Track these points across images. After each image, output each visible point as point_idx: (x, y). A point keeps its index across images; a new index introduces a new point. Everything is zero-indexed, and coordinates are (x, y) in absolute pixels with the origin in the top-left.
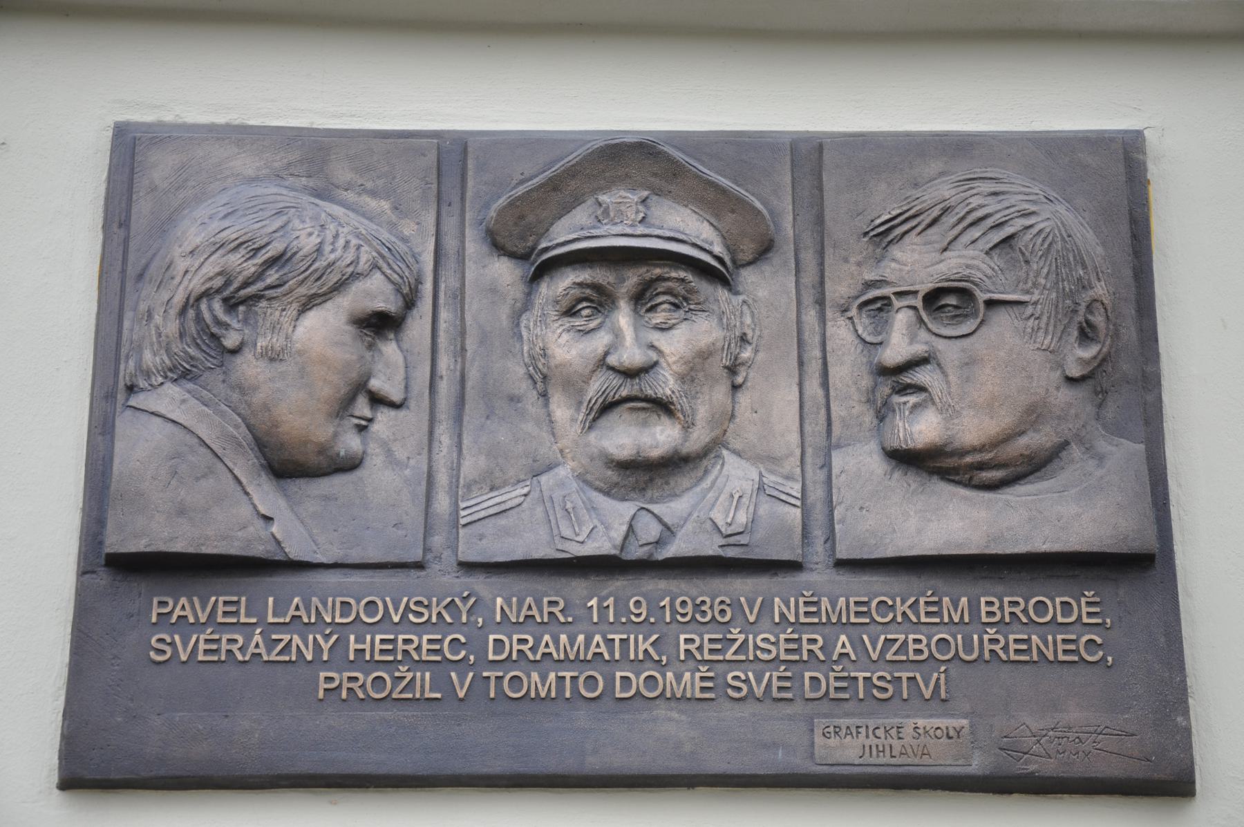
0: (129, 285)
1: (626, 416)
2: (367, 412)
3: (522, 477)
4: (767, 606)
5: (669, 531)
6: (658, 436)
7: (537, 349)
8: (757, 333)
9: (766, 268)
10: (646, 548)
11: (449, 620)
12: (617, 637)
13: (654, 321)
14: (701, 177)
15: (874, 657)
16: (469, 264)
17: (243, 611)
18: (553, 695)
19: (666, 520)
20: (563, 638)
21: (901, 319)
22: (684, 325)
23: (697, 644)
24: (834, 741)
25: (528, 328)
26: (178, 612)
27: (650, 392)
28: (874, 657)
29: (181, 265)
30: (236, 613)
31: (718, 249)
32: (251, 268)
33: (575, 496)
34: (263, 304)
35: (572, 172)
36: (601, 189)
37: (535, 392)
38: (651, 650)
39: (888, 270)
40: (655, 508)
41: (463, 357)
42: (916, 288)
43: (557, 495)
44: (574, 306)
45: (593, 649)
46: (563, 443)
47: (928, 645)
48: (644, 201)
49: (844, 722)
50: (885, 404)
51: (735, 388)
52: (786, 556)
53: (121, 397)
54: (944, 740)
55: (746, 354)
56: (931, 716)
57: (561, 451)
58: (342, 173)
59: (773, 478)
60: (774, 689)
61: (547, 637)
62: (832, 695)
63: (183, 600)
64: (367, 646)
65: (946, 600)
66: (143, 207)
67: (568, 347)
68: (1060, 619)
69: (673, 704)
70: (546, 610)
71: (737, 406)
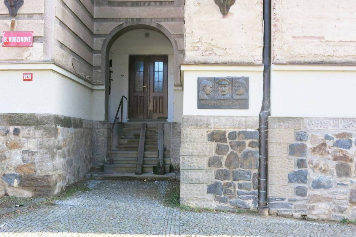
5: (225, 98)
21: (236, 87)
39: (236, 84)
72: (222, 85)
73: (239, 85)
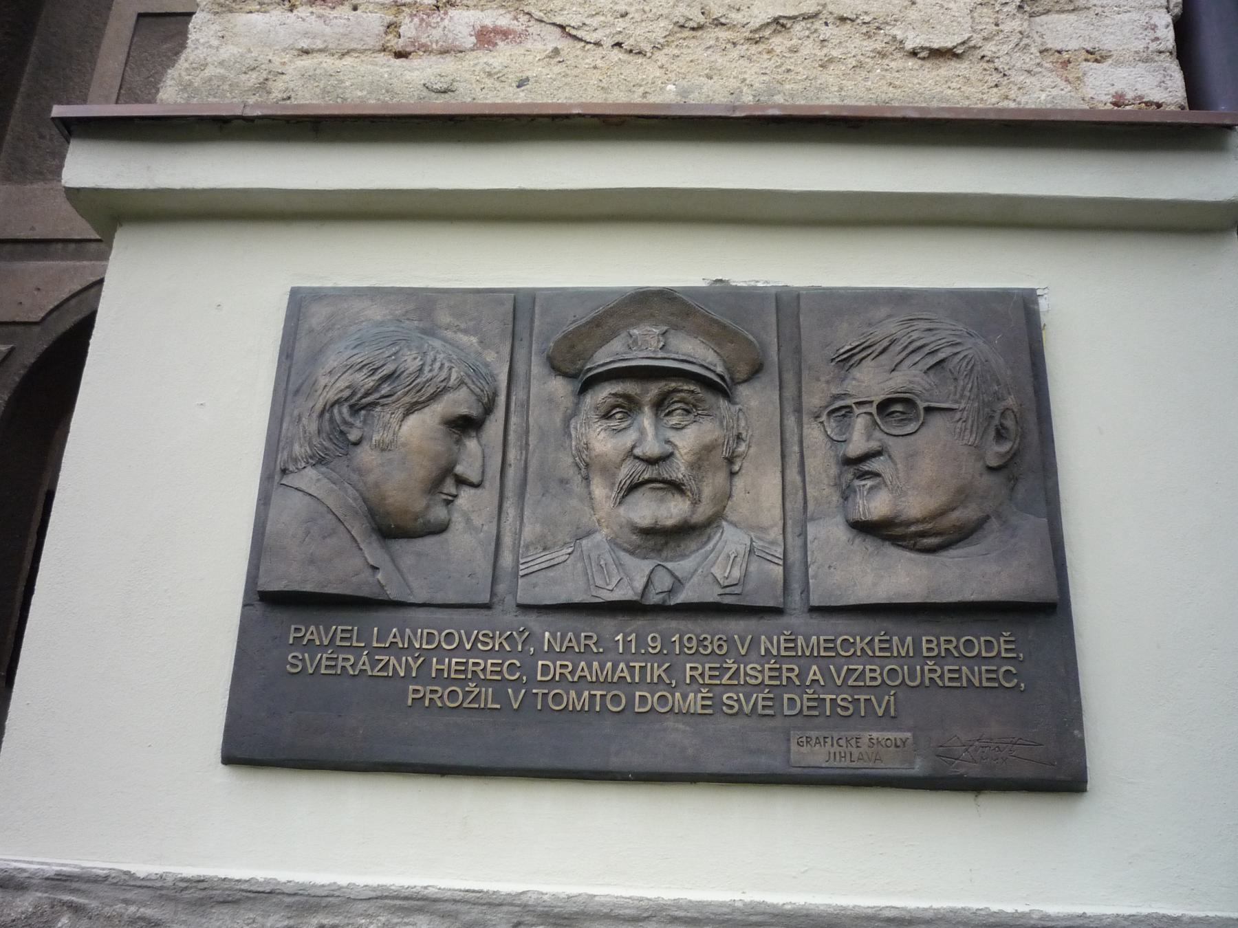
0: (289, 397)
1: (649, 494)
2: (453, 491)
4: (755, 643)
5: (678, 583)
8: (750, 433)
9: (757, 384)
10: (661, 596)
11: (508, 649)
12: (637, 665)
15: (839, 683)
16: (534, 383)
17: (355, 638)
18: (586, 708)
19: (677, 574)
20: (595, 664)
21: (860, 423)
22: (694, 427)
23: (700, 671)
24: (805, 749)
26: (308, 636)
27: (666, 476)
28: (839, 683)
29: (323, 381)
30: (350, 638)
31: (720, 369)
32: (370, 383)
33: (607, 556)
34: (379, 409)
35: (610, 313)
36: (633, 325)
38: (663, 675)
39: (850, 386)
40: (669, 565)
41: (527, 450)
42: (872, 398)
43: (594, 555)
45: (618, 674)
46: (601, 514)
47: (881, 674)
48: (664, 334)
49: (813, 734)
50: (849, 487)
52: (771, 604)
53: (277, 478)
54: (893, 748)
55: (742, 448)
56: (883, 730)
57: (599, 521)
58: (444, 318)
59: (761, 543)
60: (760, 707)
61: (583, 664)
62: (806, 712)
63: (312, 628)
64: (445, 667)
65: (895, 638)
66: (303, 345)
67: (604, 441)
68: (984, 654)
69: (680, 717)
70: (583, 641)
72: (630, 387)
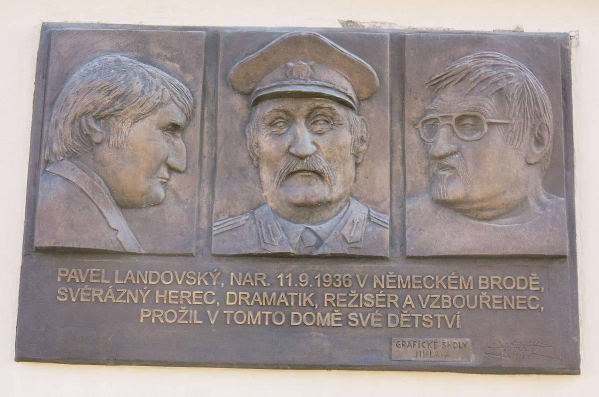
0: (47, 108)
2: (167, 176)
3: (245, 210)
4: (371, 280)
5: (320, 241)
6: (316, 191)
7: (254, 143)
11: (206, 284)
12: (293, 294)
13: (315, 130)
14: (341, 54)
15: (424, 306)
16: (220, 98)
17: (103, 277)
18: (259, 323)
19: (319, 234)
20: (265, 294)
21: (443, 132)
23: (333, 299)
24: (401, 349)
25: (249, 132)
26: (71, 276)
28: (424, 306)
29: (72, 99)
30: (100, 278)
32: (107, 100)
34: (113, 119)
37: (253, 166)
38: (310, 302)
40: (314, 228)
41: (216, 147)
42: (452, 114)
44: (274, 121)
45: (280, 300)
47: (452, 301)
49: (407, 340)
50: (434, 175)
51: (357, 165)
52: (381, 254)
53: (42, 166)
54: (458, 349)
56: (452, 337)
58: (155, 49)
60: (372, 322)
61: (256, 294)
62: (402, 325)
63: (74, 270)
64: (165, 296)
65: (462, 277)
66: (54, 69)
68: (519, 288)
69: (320, 329)
70: (256, 279)
71: (357, 175)
72: (289, 105)
73: (466, 105)
